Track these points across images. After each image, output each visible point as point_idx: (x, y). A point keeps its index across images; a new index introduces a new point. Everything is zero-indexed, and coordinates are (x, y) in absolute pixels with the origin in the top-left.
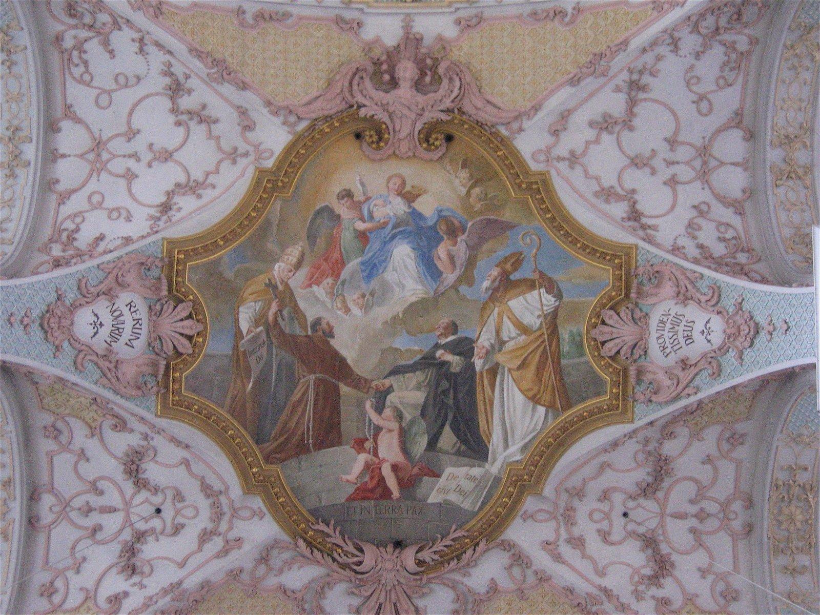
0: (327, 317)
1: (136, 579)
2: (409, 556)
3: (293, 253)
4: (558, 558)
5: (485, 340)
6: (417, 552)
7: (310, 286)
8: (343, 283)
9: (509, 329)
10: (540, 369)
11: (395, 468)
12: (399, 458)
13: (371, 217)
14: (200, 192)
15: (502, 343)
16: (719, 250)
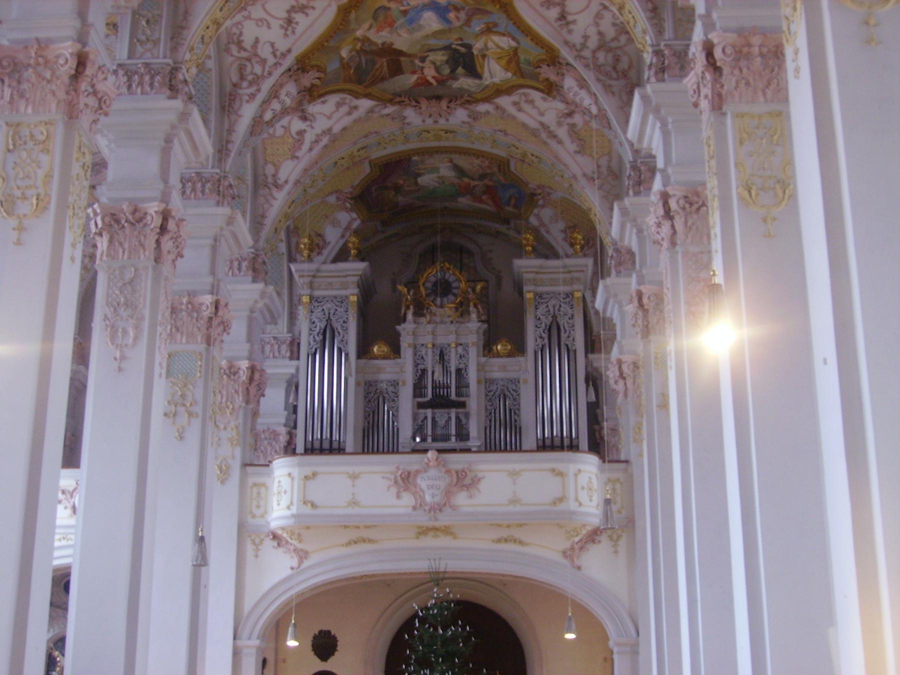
0: (388, 40)
1: (308, 123)
2: (444, 104)
3: (366, 26)
4: (520, 110)
5: (478, 46)
6: (450, 102)
7: (378, 33)
8: (396, 28)
9: (490, 44)
10: (509, 62)
11: (434, 77)
12: (436, 75)
13: (408, 4)
14: (306, 11)
15: (487, 49)
16: (610, 33)
